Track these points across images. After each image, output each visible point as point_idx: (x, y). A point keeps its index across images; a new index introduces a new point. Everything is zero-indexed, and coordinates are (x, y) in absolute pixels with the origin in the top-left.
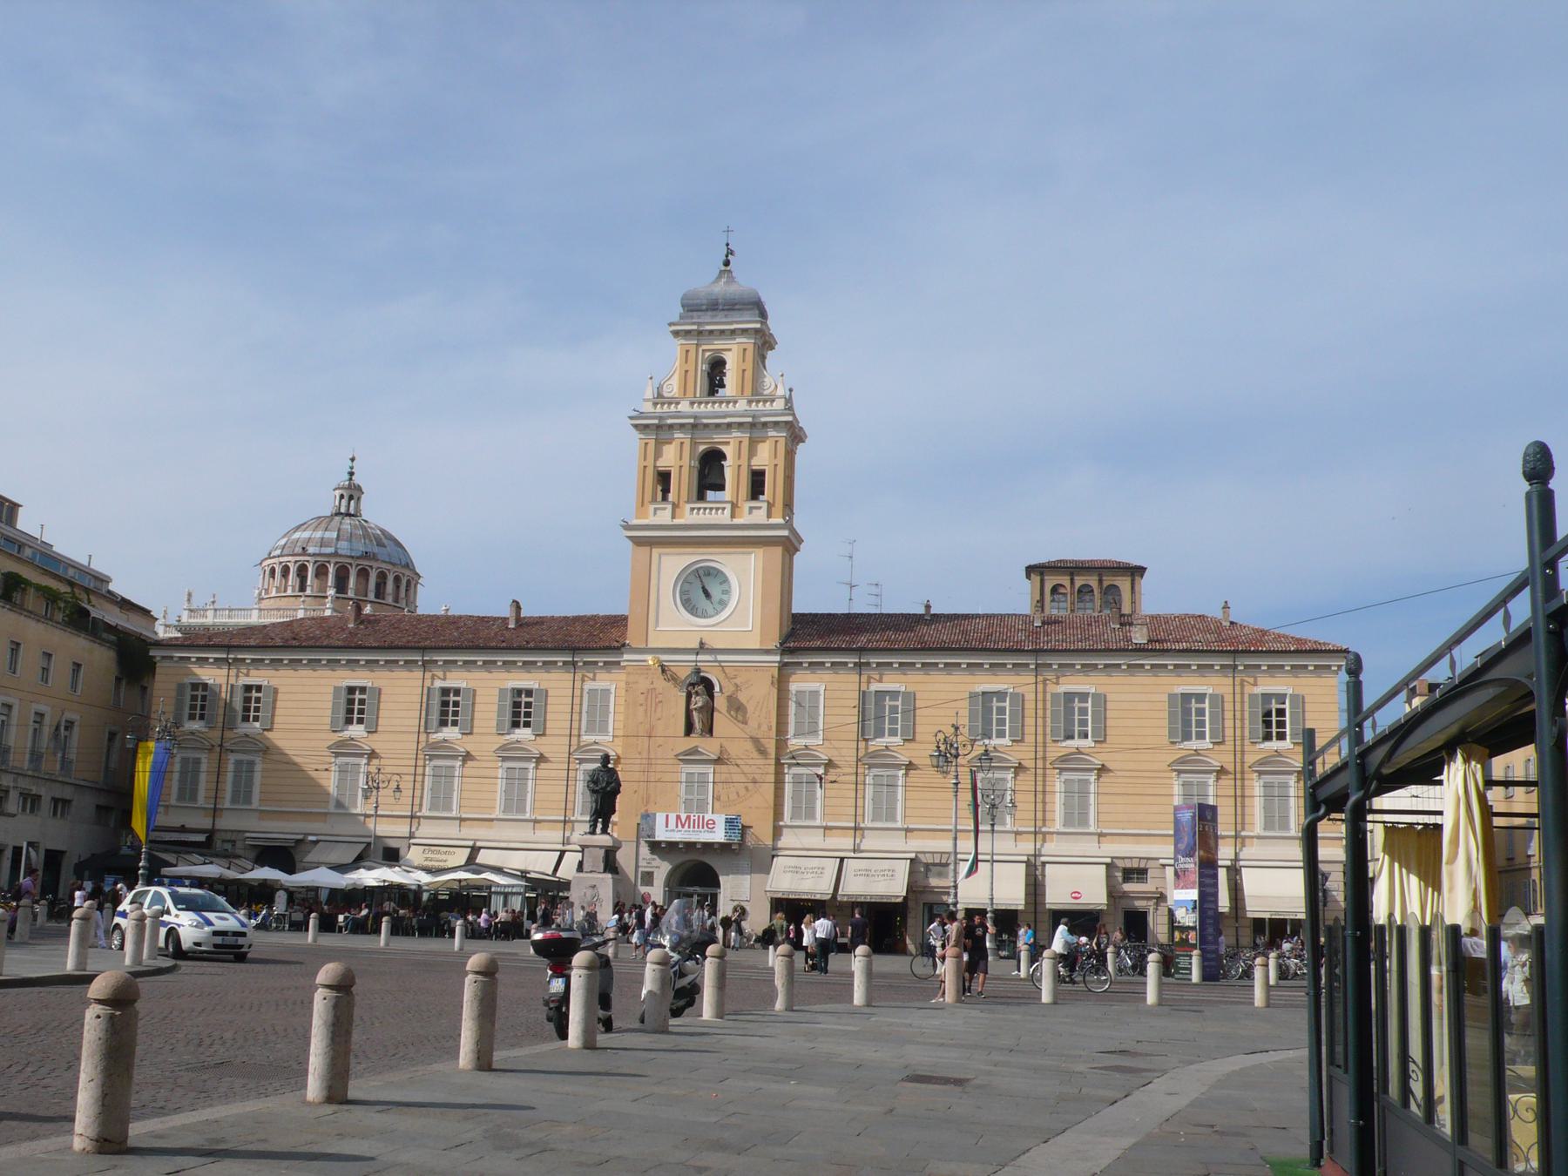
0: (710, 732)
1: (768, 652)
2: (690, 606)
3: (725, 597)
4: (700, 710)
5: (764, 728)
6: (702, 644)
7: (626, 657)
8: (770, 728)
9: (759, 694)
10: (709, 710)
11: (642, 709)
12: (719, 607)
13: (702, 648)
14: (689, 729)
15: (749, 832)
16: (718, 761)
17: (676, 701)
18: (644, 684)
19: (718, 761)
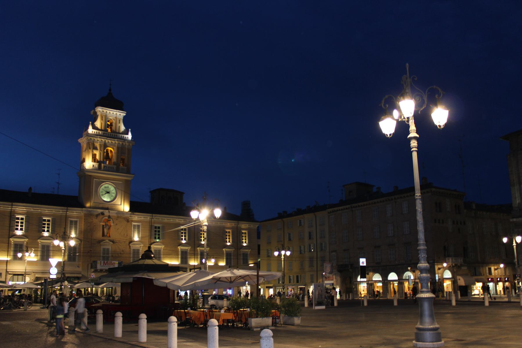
5: (125, 235)
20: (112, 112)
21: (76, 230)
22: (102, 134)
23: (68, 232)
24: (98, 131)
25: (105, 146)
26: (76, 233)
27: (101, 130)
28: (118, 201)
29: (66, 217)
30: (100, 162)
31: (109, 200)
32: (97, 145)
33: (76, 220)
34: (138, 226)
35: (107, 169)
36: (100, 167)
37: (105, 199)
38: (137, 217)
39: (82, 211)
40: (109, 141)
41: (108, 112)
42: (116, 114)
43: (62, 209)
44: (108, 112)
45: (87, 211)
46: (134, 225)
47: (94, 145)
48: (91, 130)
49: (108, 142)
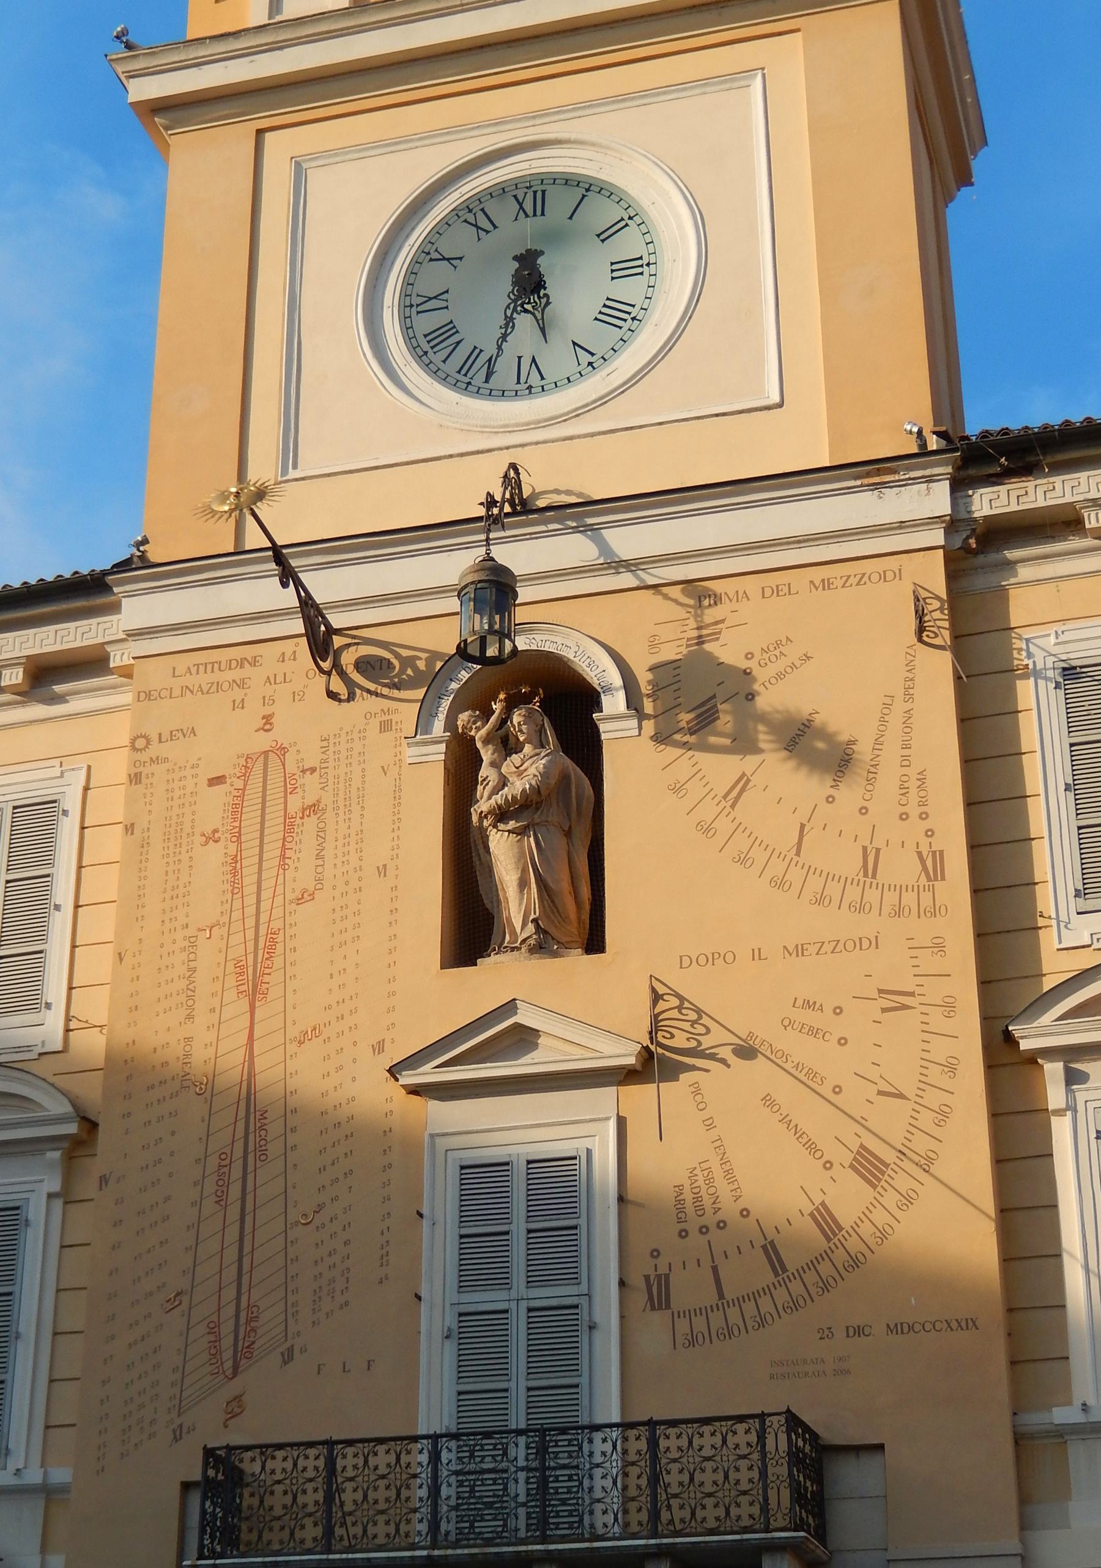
0: (595, 943)
1: (875, 471)
2: (472, 371)
3: (629, 290)
4: (520, 812)
5: (901, 868)
6: (512, 478)
7: (139, 608)
8: (933, 868)
9: (860, 656)
10: (573, 817)
11: (214, 857)
12: (600, 337)
13: (515, 506)
14: (471, 931)
15: (851, 1478)
16: (651, 1066)
17: (390, 777)
18: (224, 735)
19: (651, 1066)
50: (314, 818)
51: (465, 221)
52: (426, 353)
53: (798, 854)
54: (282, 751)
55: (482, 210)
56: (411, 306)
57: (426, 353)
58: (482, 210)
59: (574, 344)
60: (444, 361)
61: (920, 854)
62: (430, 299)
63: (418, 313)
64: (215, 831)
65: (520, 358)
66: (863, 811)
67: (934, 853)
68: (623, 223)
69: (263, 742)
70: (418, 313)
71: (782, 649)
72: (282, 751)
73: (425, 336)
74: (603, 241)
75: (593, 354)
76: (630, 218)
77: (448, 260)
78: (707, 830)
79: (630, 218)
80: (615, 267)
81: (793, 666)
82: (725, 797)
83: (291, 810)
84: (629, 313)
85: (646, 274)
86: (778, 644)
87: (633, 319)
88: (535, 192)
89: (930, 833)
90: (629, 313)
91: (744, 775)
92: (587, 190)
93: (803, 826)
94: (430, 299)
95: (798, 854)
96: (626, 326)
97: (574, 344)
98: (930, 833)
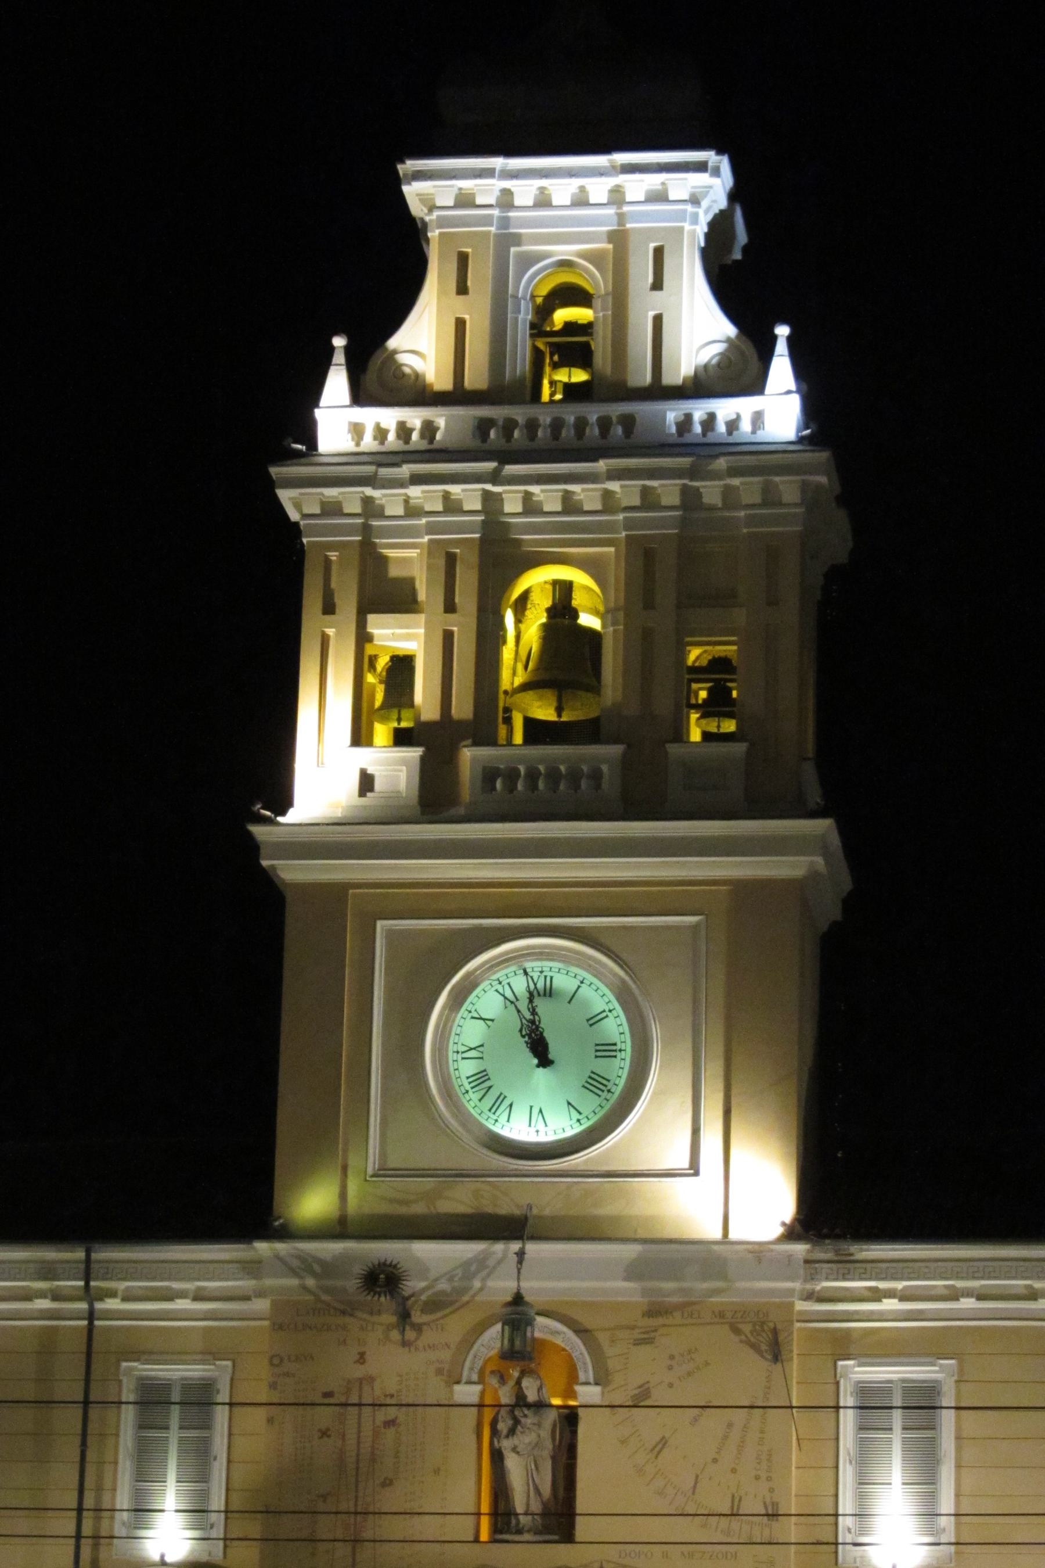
20: (562, 191)
21: (198, 1471)
22: (471, 442)
23: (123, 1500)
24: (415, 417)
25: (500, 557)
26: (197, 1511)
27: (456, 396)
28: (660, 1130)
29: (92, 1346)
30: (434, 743)
31: (558, 1125)
32: (408, 557)
33: (195, 1371)
34: (922, 1404)
35: (515, 797)
36: (435, 796)
37: (517, 1128)
38: (902, 1294)
39: (252, 1268)
40: (528, 496)
41: (524, 192)
42: (617, 197)
43: (47, 1272)
44: (524, 192)
45: (306, 1266)
46: (872, 1404)
47: (370, 559)
48: (339, 421)
49: (530, 507)
50: (392, 1430)
51: (497, 991)
52: (467, 1092)
53: (693, 1493)
54: (371, 1379)
55: (509, 984)
56: (458, 1052)
57: (467, 1092)
58: (509, 984)
59: (569, 1104)
60: (480, 1100)
61: (765, 1503)
62: (471, 1049)
63: (463, 1058)
64: (328, 1429)
65: (531, 1107)
66: (734, 1471)
67: (773, 1504)
68: (604, 1014)
69: (359, 1372)
70: (463, 1058)
71: (693, 1356)
72: (371, 1379)
73: (468, 1078)
74: (591, 1025)
75: (580, 1113)
76: (610, 1011)
77: (484, 1020)
78: (640, 1471)
79: (610, 1011)
80: (598, 1048)
81: (698, 1368)
82: (652, 1450)
83: (378, 1423)
84: (606, 1086)
85: (619, 1057)
86: (690, 1352)
87: (609, 1091)
88: (546, 977)
89: (771, 1490)
90: (606, 1086)
91: (664, 1437)
92: (582, 982)
93: (697, 1477)
94: (471, 1049)
95: (693, 1493)
96: (605, 1094)
97: (569, 1104)
98: (771, 1490)
